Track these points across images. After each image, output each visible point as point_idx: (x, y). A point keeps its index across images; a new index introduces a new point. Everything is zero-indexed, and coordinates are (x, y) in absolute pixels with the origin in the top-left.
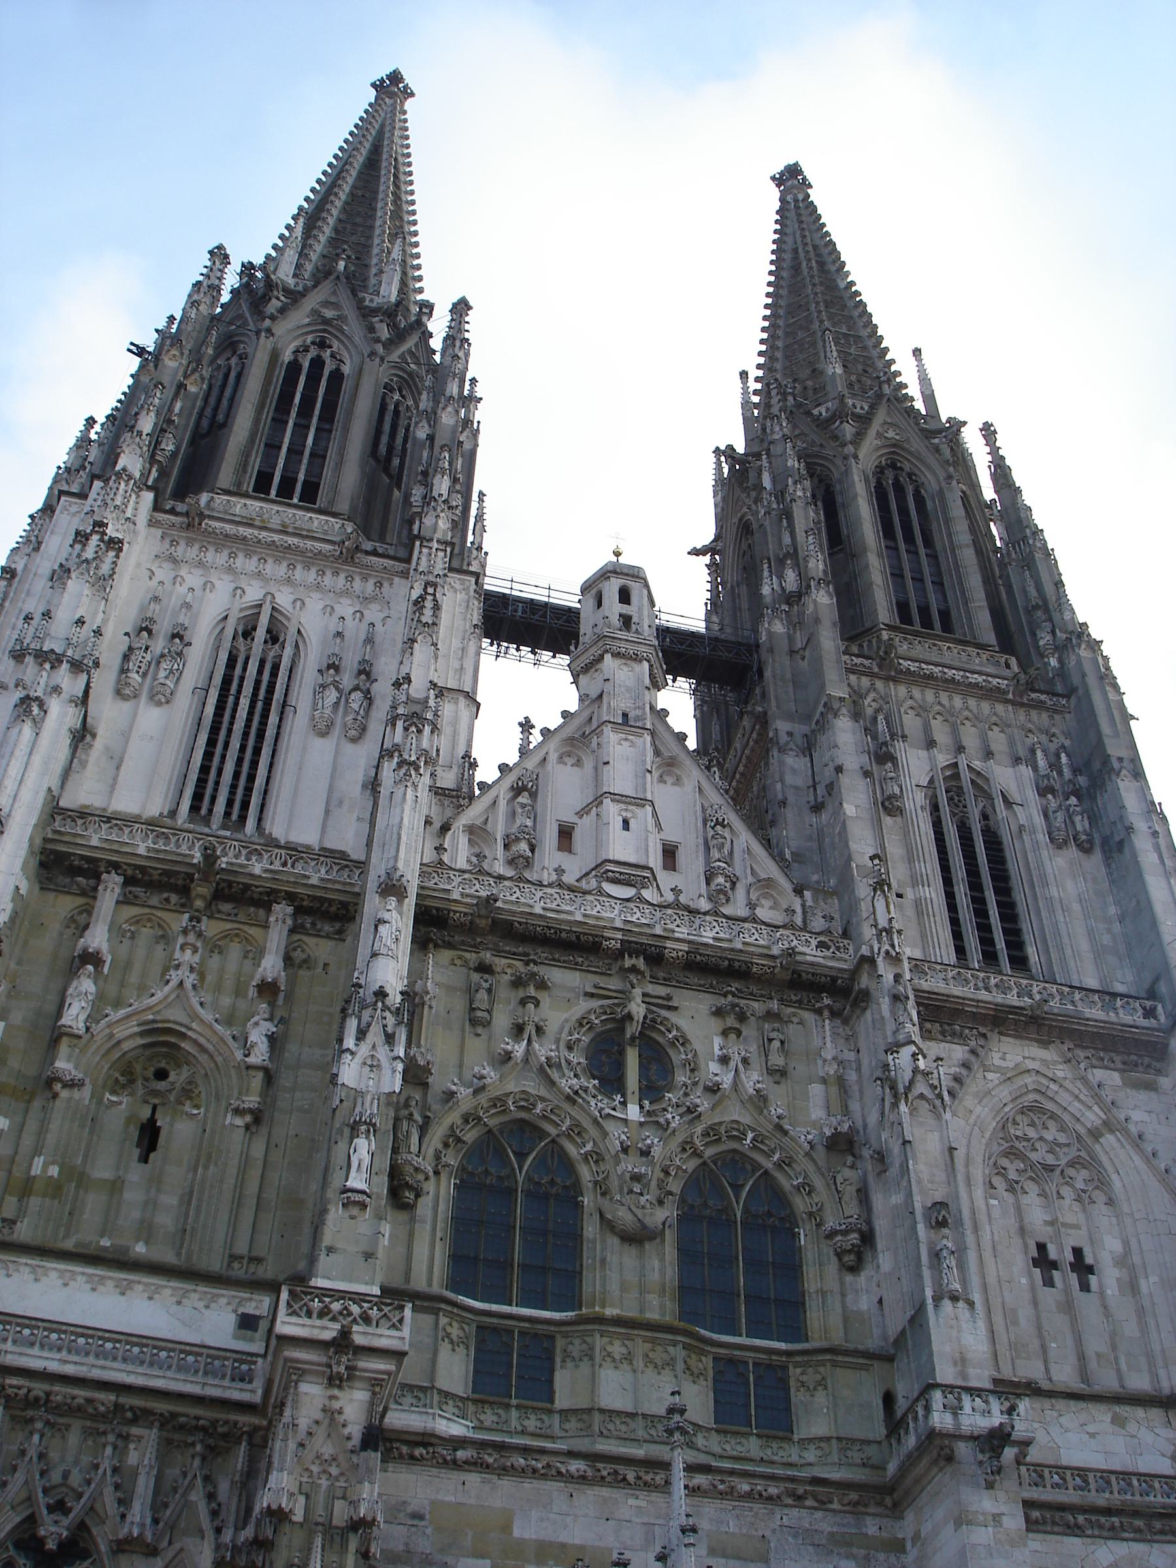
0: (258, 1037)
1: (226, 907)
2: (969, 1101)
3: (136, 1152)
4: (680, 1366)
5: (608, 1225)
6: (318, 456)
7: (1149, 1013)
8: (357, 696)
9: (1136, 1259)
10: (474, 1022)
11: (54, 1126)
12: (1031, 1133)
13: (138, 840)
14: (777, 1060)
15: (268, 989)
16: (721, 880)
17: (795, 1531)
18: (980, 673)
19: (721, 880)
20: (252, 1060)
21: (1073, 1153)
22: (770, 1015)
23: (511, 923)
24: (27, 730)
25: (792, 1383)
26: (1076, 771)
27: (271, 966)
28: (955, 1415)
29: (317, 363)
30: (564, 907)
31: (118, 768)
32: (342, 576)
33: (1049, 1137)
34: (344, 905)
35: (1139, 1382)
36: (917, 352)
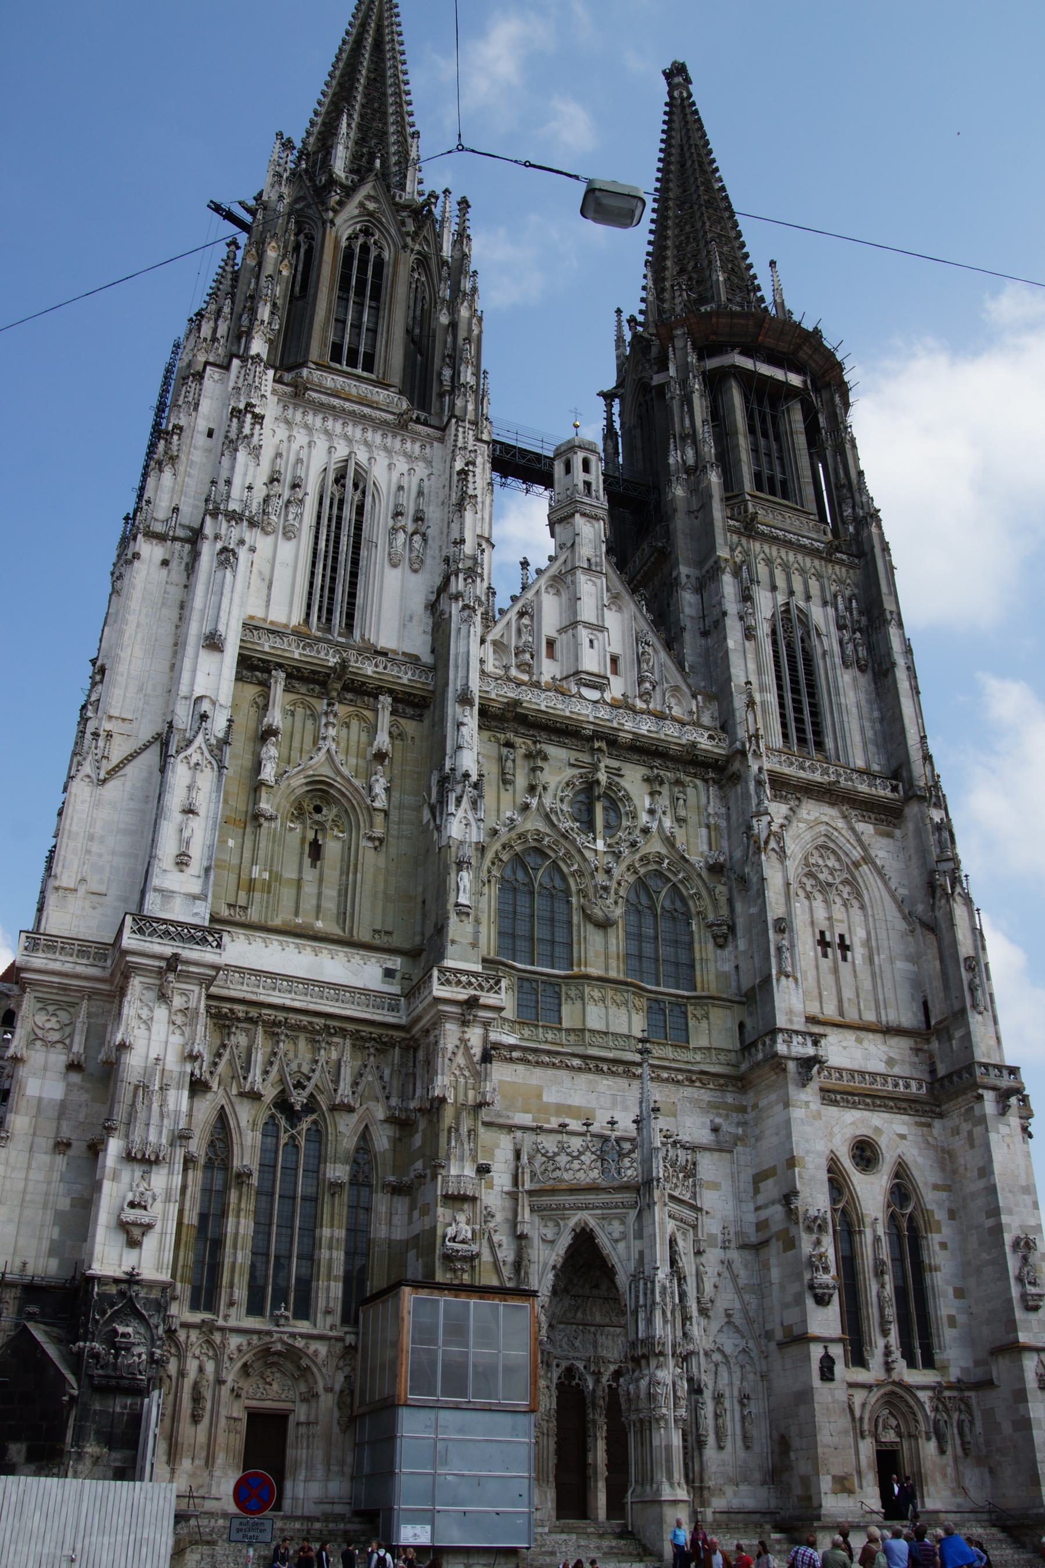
0: (379, 789)
1: (349, 696)
3: (307, 861)
4: (630, 1005)
5: (588, 918)
6: (373, 331)
7: (894, 789)
8: (417, 538)
9: (874, 943)
10: (505, 782)
11: (263, 845)
12: (821, 862)
13: (293, 648)
15: (380, 756)
16: (647, 685)
17: (691, 1100)
18: (808, 538)
19: (647, 685)
20: (377, 804)
22: (678, 782)
23: (526, 716)
24: (228, 573)
25: (690, 1016)
26: (861, 613)
27: (383, 741)
28: (789, 1047)
29: (365, 249)
30: (559, 706)
31: (270, 587)
32: (399, 438)
33: (830, 864)
34: (424, 698)
35: (870, 1016)
36: (773, 264)
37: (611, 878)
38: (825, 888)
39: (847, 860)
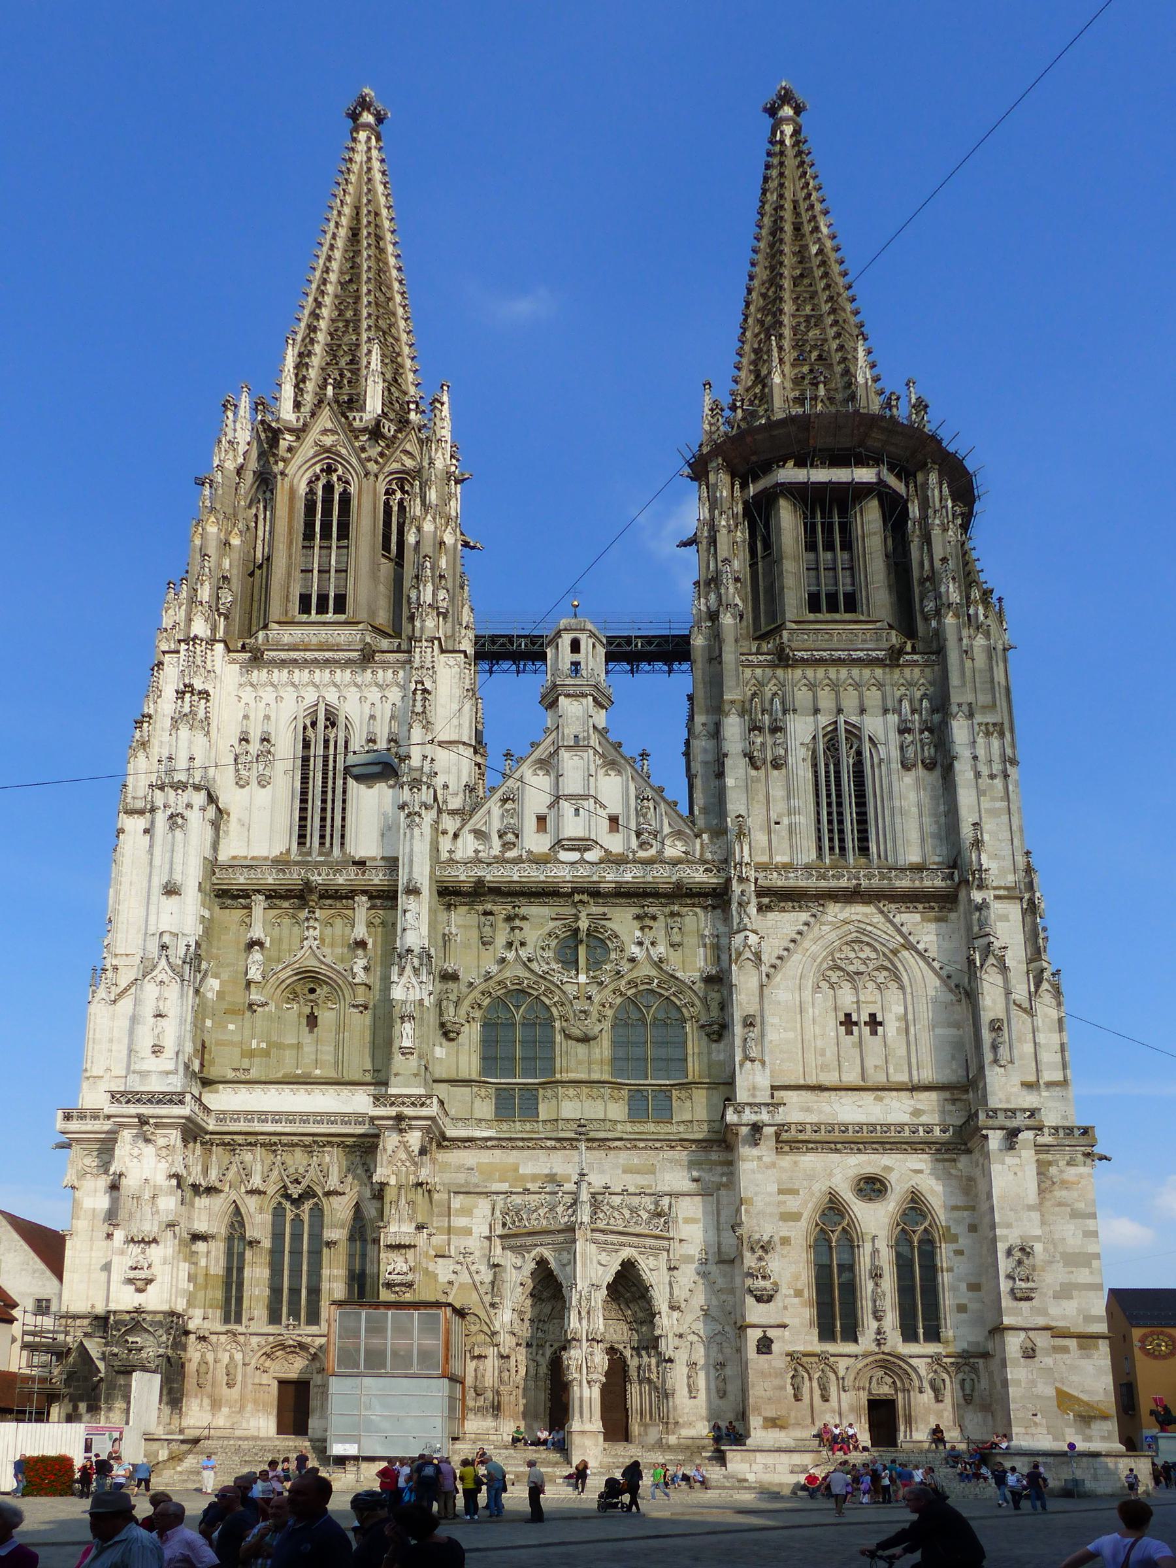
1: (329, 902)
2: (806, 943)
9: (910, 1017)
10: (484, 944)
12: (852, 955)
14: (676, 939)
16: (645, 836)
21: (877, 963)
22: (673, 914)
37: (592, 1003)
38: (852, 977)
39: (884, 949)
